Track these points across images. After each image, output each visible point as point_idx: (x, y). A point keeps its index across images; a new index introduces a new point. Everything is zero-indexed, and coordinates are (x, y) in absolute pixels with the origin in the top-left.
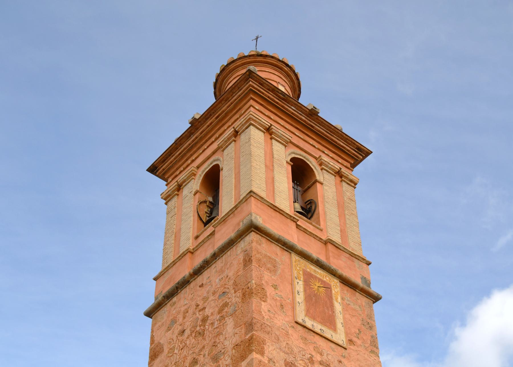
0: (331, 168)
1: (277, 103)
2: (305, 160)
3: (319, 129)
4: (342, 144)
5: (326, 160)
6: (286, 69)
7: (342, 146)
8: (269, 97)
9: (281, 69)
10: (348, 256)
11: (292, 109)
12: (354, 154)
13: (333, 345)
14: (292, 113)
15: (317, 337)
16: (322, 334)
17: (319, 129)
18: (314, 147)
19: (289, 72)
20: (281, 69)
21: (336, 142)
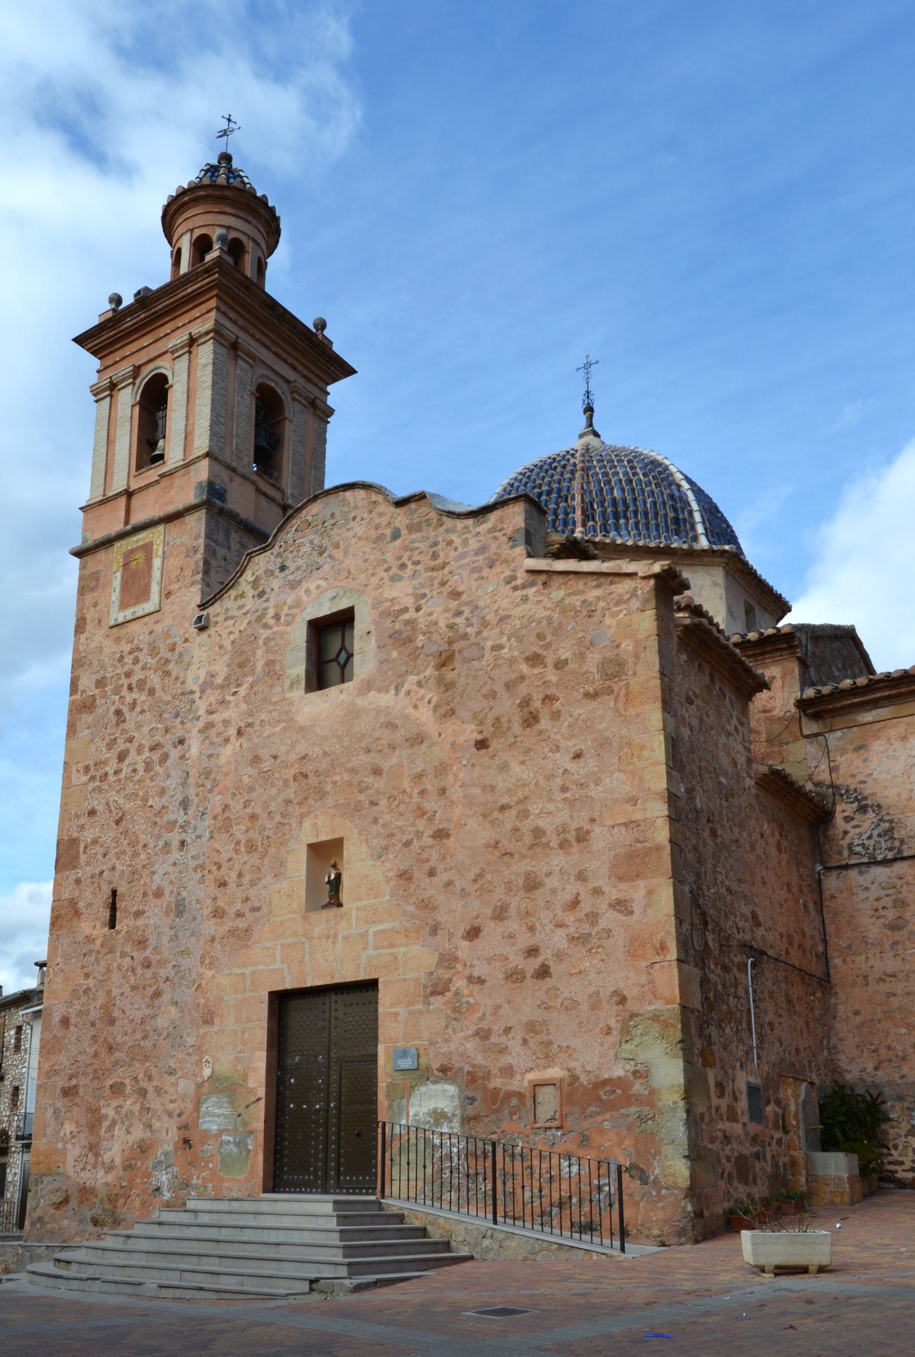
0: (182, 347)
1: (115, 335)
2: (153, 373)
3: (160, 307)
4: (189, 290)
5: (171, 345)
6: (186, 199)
7: (193, 291)
8: (106, 340)
9: (185, 204)
10: (183, 471)
11: (129, 323)
12: (208, 283)
13: (146, 619)
14: (132, 325)
15: (130, 625)
16: (134, 617)
17: (160, 307)
18: (167, 334)
19: (192, 196)
20: (185, 204)
21: (184, 297)
